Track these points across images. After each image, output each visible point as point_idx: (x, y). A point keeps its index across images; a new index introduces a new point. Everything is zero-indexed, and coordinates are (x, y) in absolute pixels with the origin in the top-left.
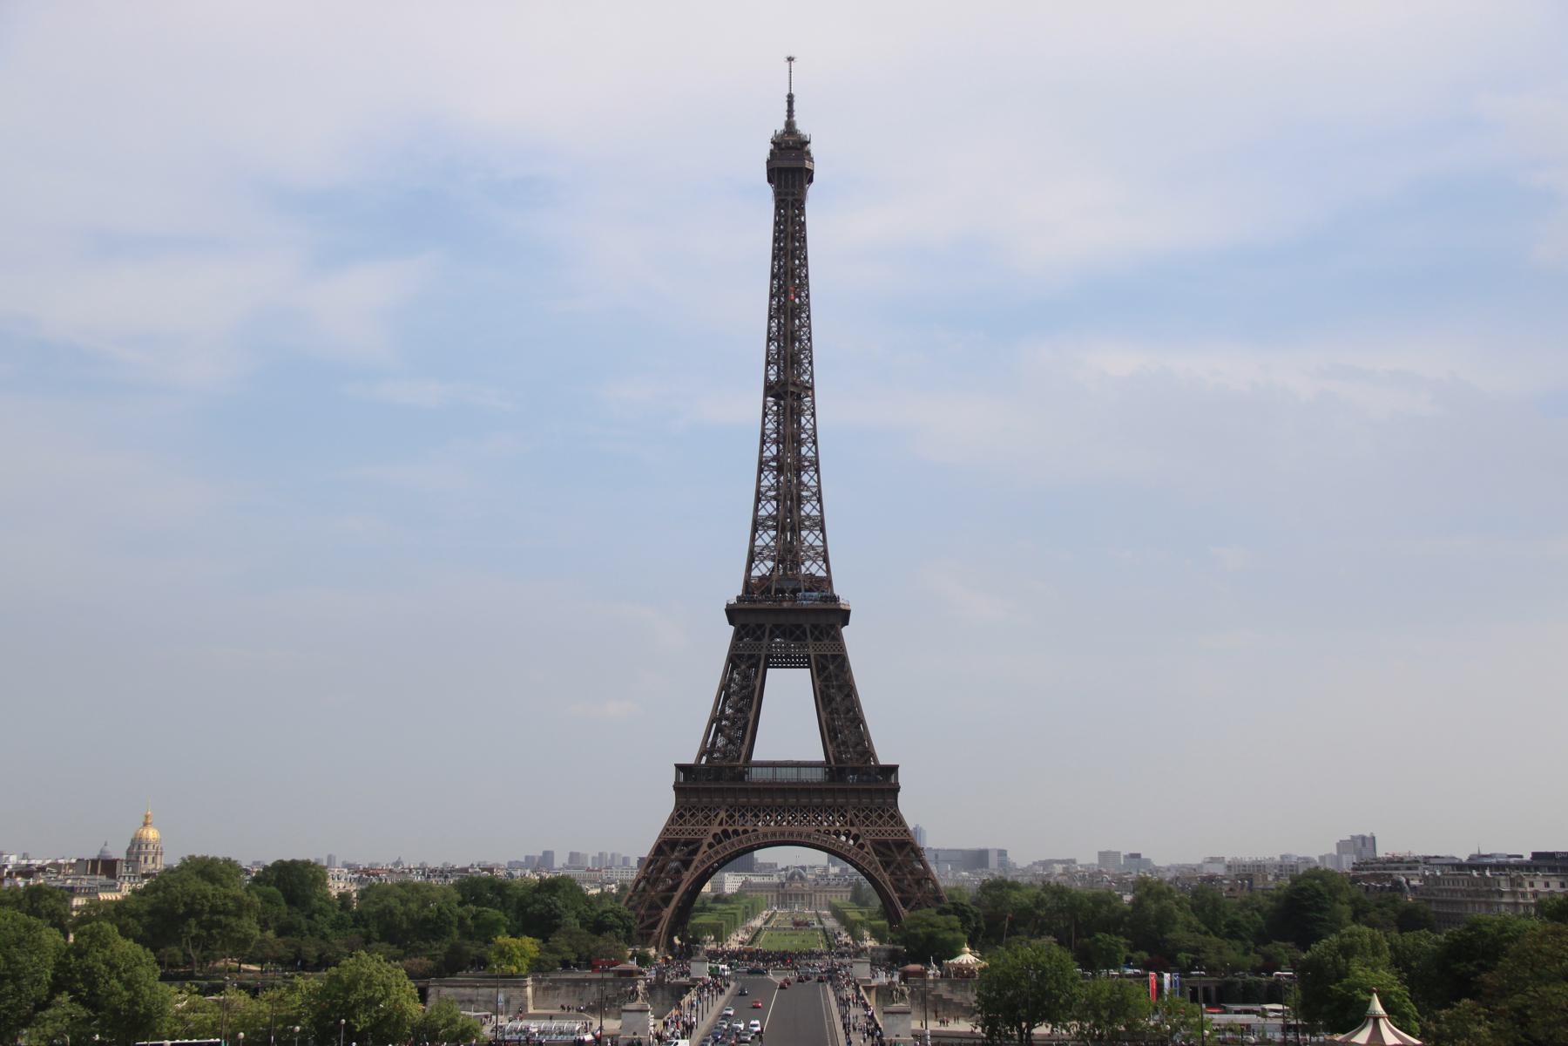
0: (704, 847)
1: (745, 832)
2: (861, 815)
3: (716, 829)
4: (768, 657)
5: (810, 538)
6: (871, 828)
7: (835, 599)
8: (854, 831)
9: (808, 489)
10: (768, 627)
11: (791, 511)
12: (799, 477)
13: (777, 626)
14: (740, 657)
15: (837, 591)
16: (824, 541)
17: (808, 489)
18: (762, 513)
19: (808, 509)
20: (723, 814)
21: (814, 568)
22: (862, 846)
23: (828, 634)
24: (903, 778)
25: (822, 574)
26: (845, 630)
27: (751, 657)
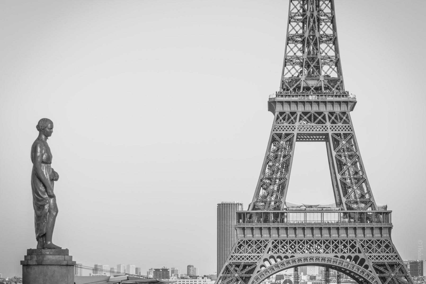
0: (258, 269)
1: (286, 257)
2: (366, 246)
3: (266, 255)
4: (298, 134)
5: (326, 49)
6: (374, 254)
7: (346, 94)
8: (361, 256)
9: (325, 15)
10: (298, 114)
11: (313, 29)
12: (318, 6)
13: (305, 113)
14: (280, 136)
15: (347, 88)
16: (337, 51)
17: (325, 15)
18: (293, 32)
19: (326, 29)
20: (270, 246)
21: (328, 70)
22: (367, 267)
23: (341, 119)
24: (394, 219)
25: (334, 75)
26: (351, 113)
27: (287, 135)
